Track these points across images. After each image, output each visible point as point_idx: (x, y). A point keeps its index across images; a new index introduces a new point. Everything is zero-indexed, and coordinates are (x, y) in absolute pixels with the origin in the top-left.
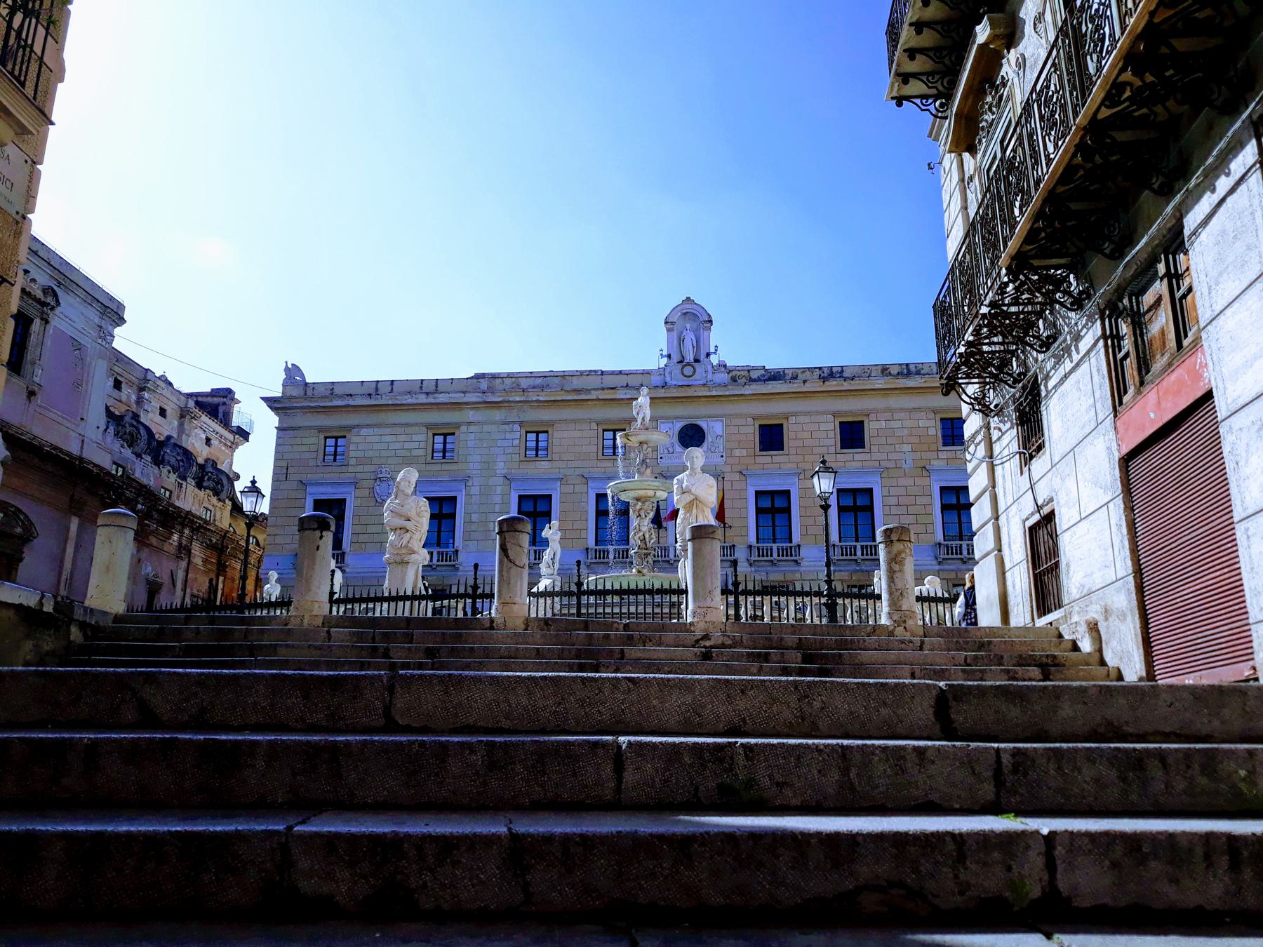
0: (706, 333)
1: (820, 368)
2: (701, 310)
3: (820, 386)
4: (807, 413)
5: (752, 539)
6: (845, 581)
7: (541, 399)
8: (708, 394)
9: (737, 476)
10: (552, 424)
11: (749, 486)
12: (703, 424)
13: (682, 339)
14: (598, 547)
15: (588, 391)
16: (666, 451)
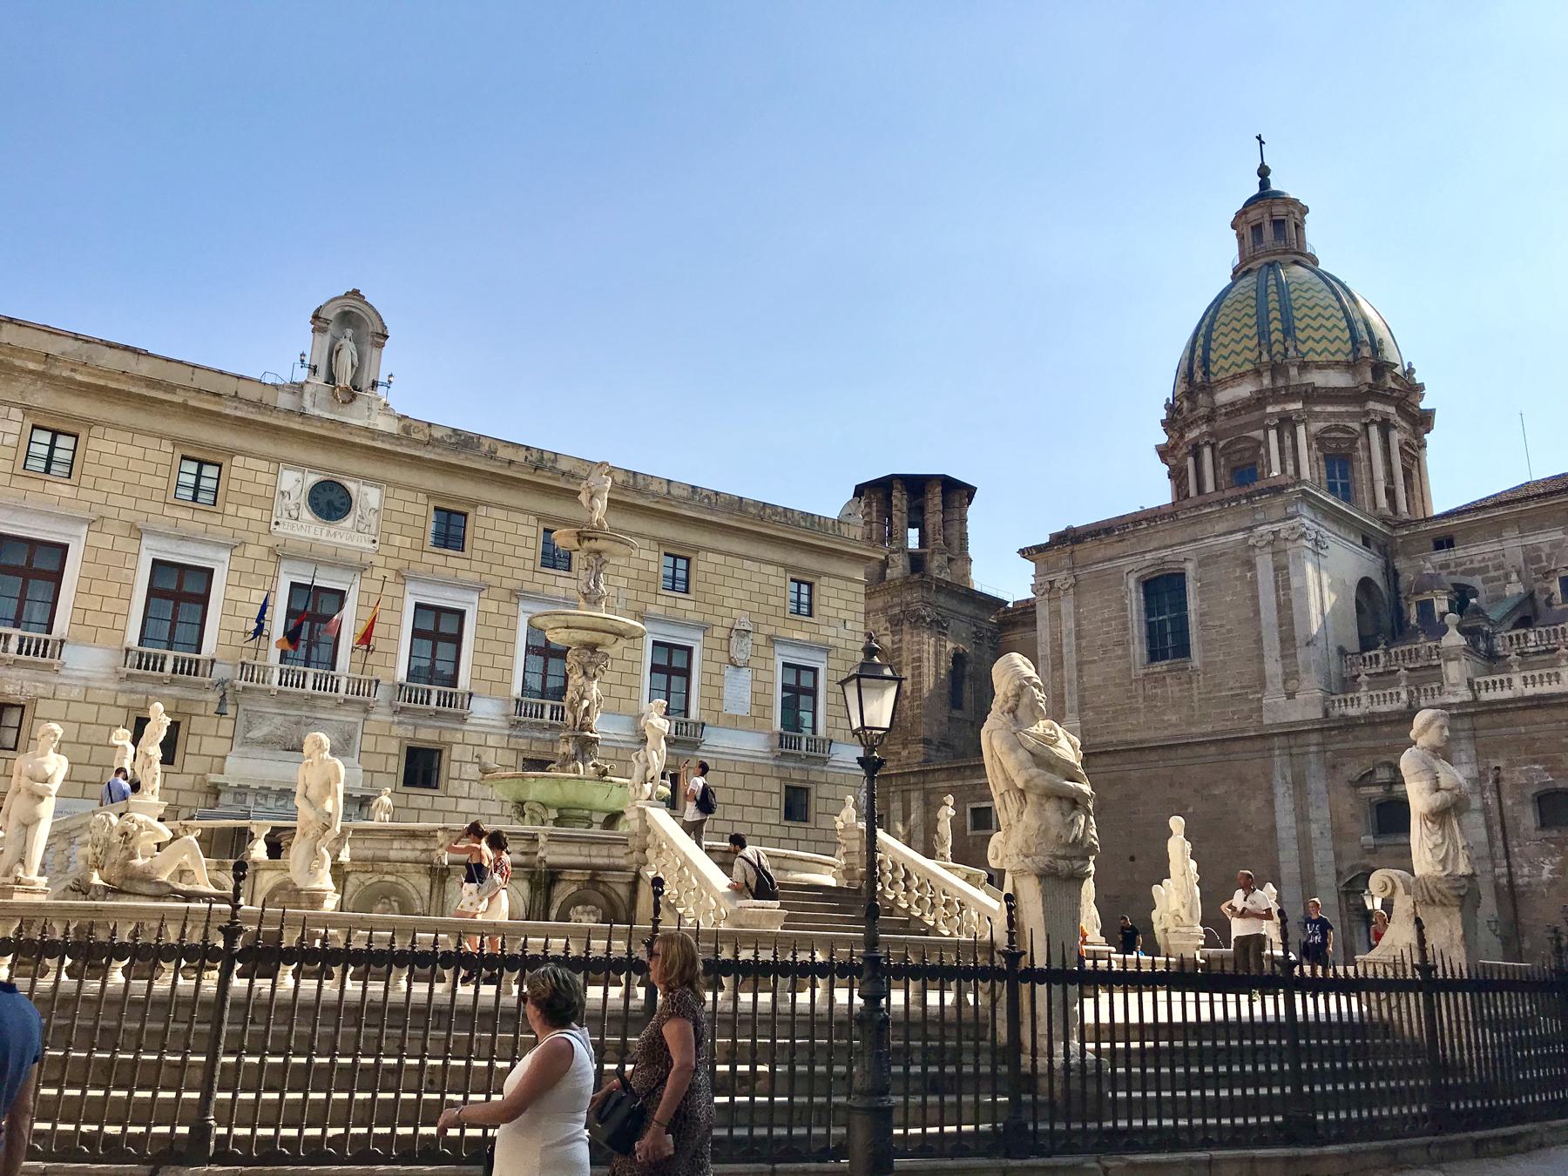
0: (375, 352)
1: (528, 448)
2: (373, 316)
3: (529, 473)
4: (502, 507)
5: (401, 674)
6: (522, 751)
7: (79, 377)
8: (370, 443)
9: (391, 576)
10: (90, 423)
11: (407, 593)
12: (352, 486)
13: (337, 347)
14: (146, 650)
15: (172, 388)
16: (286, 514)
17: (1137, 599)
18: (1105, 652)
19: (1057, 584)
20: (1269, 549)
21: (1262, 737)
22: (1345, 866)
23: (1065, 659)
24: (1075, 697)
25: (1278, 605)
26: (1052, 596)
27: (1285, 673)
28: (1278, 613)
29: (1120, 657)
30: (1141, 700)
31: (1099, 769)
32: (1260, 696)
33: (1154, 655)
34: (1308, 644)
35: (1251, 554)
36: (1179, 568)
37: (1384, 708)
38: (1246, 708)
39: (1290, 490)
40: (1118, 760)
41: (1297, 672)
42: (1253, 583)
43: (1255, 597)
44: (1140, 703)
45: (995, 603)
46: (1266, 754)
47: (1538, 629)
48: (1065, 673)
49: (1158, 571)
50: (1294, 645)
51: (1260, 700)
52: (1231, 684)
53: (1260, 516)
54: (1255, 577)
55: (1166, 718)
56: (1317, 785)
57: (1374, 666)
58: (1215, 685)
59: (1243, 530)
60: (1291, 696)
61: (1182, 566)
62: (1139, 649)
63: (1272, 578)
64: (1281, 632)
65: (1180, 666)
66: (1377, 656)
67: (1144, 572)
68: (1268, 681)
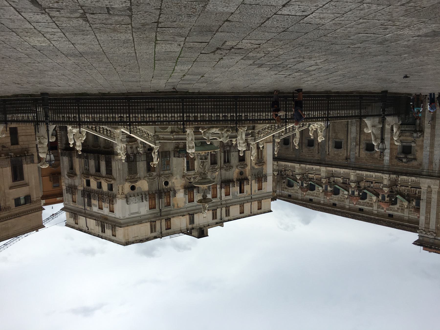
20: (430, 230)
22: (421, 138)
25: (430, 214)
28: (430, 211)
34: (422, 200)
37: (405, 177)
39: (418, 243)
41: (427, 193)
42: (437, 223)
43: (437, 218)
50: (427, 200)
53: (431, 241)
56: (426, 161)
57: (420, 191)
59: (438, 240)
60: (429, 187)
63: (431, 221)
68: (437, 193)
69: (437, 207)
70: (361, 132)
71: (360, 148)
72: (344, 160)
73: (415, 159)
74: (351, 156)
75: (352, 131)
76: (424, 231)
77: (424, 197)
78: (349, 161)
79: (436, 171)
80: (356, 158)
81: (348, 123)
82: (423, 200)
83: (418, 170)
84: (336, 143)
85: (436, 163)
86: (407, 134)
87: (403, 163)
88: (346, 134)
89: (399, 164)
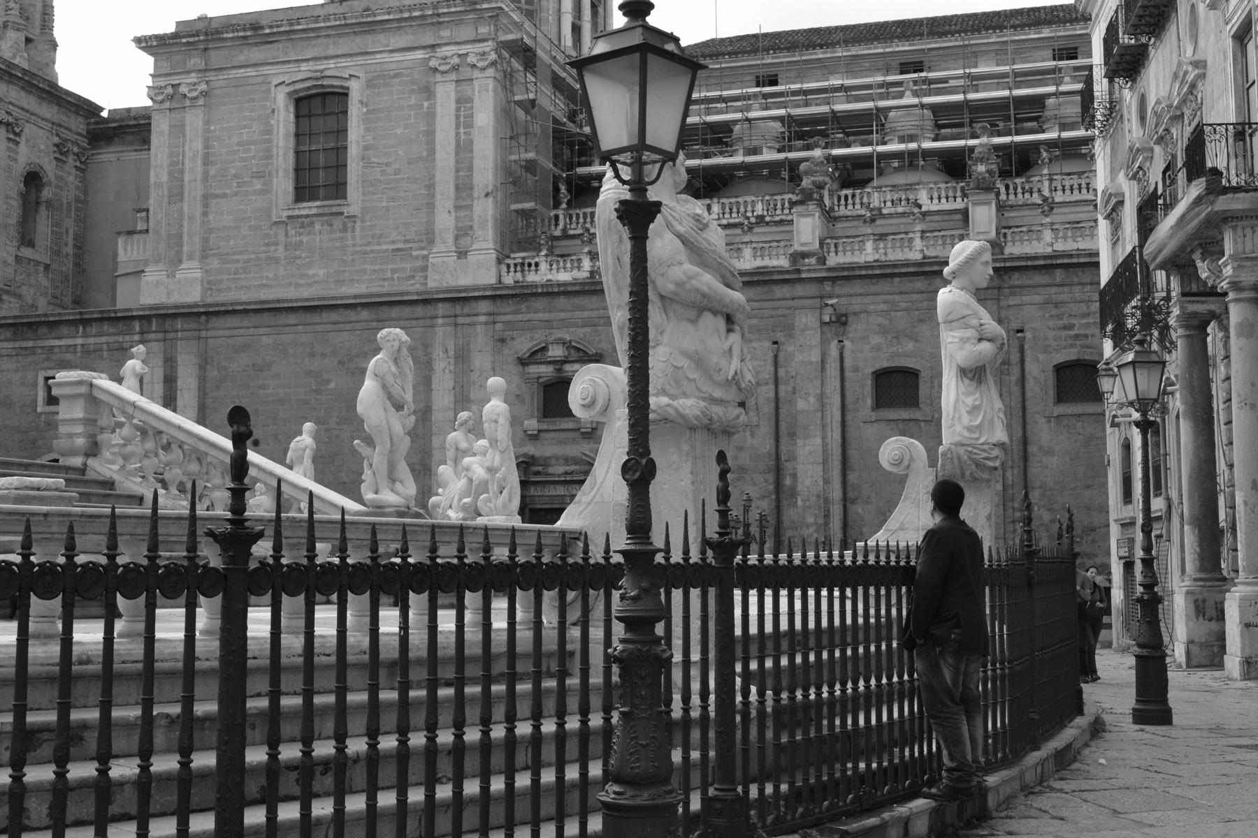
17: (285, 120)
18: (239, 185)
19: (183, 89)
20: (453, 76)
21: (426, 302)
23: (186, 190)
24: (197, 239)
26: (175, 105)
27: (458, 228)
28: (457, 154)
29: (259, 193)
30: (281, 248)
31: (221, 333)
32: (425, 252)
33: (303, 192)
34: (487, 195)
35: (431, 79)
36: (342, 87)
37: (564, 277)
38: (408, 266)
40: (246, 322)
41: (471, 227)
42: (431, 115)
43: (431, 133)
44: (281, 252)
45: (87, 109)
46: (428, 322)
47: (722, 201)
48: (186, 208)
49: (315, 87)
50: (471, 196)
51: (425, 257)
52: (393, 236)
53: (446, 33)
54: (433, 106)
55: (311, 272)
57: (553, 228)
58: (373, 236)
59: (424, 48)
60: (462, 254)
61: (346, 84)
62: (284, 184)
64: (457, 178)
65: (334, 210)
66: (557, 217)
67: (298, 86)
69: (434, 176)
70: (772, 463)
71: (772, 387)
72: (856, 314)
73: (523, 362)
74: (813, 337)
75: (820, 468)
76: (474, 66)
77: (485, 211)
78: (829, 310)
79: (443, 325)
80: (789, 329)
81: (845, 507)
82: (483, 194)
83: (508, 318)
84: (911, 399)
85: (445, 356)
86: (561, 469)
87: (568, 338)
88: (852, 452)
89: (587, 330)
